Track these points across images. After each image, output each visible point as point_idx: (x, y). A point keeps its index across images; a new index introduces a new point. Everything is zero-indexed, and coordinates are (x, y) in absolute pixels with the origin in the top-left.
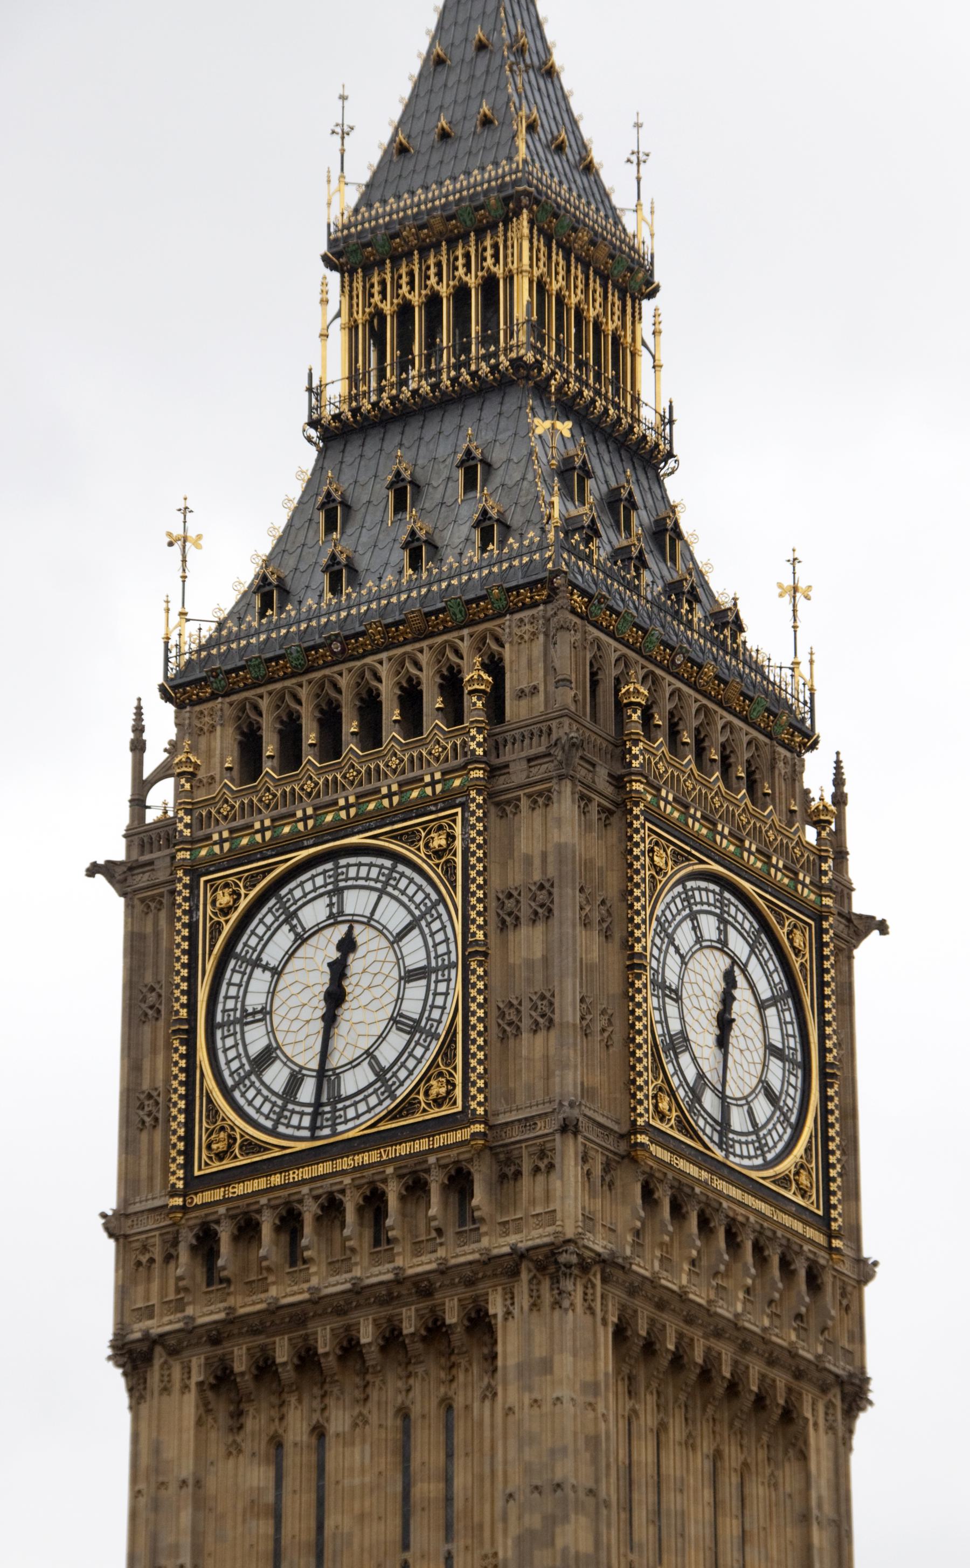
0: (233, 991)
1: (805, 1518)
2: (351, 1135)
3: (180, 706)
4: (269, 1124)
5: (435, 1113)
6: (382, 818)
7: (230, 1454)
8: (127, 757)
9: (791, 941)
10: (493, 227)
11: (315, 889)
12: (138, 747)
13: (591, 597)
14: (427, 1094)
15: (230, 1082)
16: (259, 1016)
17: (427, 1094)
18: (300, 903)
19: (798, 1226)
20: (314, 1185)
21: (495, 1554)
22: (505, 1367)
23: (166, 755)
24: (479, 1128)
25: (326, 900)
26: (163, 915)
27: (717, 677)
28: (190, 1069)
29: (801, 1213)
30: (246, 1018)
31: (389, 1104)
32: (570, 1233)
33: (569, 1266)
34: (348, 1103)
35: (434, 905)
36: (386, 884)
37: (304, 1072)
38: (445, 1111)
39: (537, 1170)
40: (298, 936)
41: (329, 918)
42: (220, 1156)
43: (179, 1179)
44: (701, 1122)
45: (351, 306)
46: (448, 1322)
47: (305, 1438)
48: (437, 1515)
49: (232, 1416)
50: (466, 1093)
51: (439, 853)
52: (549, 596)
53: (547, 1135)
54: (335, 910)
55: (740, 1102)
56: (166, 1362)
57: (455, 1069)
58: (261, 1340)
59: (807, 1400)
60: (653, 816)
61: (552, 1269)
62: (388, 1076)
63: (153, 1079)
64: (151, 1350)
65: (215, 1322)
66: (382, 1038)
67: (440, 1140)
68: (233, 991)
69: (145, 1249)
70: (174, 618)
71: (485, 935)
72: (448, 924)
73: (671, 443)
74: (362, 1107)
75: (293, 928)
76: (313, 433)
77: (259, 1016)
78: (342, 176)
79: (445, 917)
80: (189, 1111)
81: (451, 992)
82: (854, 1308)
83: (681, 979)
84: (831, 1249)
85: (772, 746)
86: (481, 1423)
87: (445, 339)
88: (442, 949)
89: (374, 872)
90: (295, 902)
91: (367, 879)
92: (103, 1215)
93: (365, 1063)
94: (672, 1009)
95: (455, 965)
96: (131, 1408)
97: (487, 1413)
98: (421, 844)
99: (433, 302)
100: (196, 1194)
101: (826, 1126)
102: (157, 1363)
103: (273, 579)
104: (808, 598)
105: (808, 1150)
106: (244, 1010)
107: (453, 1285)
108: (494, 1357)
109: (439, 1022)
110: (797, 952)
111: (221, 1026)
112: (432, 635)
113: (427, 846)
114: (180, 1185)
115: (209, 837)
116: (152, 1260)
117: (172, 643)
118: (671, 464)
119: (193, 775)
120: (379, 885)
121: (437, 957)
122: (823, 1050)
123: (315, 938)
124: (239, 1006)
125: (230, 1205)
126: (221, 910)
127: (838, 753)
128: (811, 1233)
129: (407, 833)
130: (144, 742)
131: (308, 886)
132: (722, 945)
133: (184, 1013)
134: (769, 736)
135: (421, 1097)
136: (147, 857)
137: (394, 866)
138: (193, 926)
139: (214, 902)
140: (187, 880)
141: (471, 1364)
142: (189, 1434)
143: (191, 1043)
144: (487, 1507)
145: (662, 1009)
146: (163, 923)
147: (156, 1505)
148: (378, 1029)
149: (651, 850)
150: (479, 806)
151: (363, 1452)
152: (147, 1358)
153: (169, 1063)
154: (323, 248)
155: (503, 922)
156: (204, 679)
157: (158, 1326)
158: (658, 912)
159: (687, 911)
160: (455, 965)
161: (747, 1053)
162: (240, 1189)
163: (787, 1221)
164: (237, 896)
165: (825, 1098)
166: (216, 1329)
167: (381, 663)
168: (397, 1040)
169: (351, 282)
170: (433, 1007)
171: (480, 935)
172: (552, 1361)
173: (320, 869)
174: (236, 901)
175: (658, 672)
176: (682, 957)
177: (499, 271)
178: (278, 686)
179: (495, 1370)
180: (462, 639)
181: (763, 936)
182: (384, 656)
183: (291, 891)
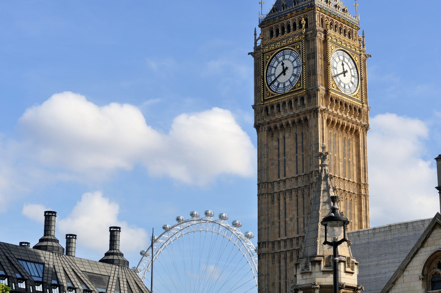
0: (269, 71)
3: (261, 28)
4: (275, 91)
5: (298, 89)
8: (254, 36)
9: (355, 59)
11: (281, 55)
12: (255, 34)
13: (321, 8)
14: (297, 86)
16: (273, 75)
17: (297, 86)
19: (357, 103)
21: (309, 154)
22: (310, 126)
24: (305, 91)
28: (264, 83)
29: (357, 101)
30: (271, 75)
31: (292, 87)
34: (286, 87)
35: (298, 57)
36: (291, 54)
38: (300, 88)
39: (314, 96)
40: (278, 62)
42: (268, 96)
44: (340, 88)
47: (282, 138)
49: (272, 135)
50: (303, 86)
51: (298, 49)
53: (315, 91)
56: (262, 127)
57: (301, 82)
60: (331, 41)
61: (316, 112)
63: (259, 85)
64: (260, 125)
65: (268, 121)
66: (291, 77)
67: (299, 93)
68: (269, 71)
69: (258, 110)
70: (260, 15)
71: (305, 61)
72: (300, 60)
74: (288, 88)
75: (278, 61)
77: (273, 75)
79: (299, 59)
80: (263, 90)
83: (337, 66)
85: (353, 29)
86: (307, 134)
88: (299, 63)
90: (278, 57)
91: (288, 53)
92: (252, 106)
95: (301, 66)
96: (257, 134)
98: (296, 47)
102: (261, 127)
103: (275, 8)
106: (271, 74)
109: (299, 74)
110: (356, 61)
111: (268, 76)
113: (296, 48)
114: (262, 101)
115: (265, 48)
116: (259, 112)
117: (260, 18)
119: (263, 39)
120: (290, 54)
122: (361, 76)
128: (359, 103)
130: (256, 34)
131: (280, 55)
133: (262, 75)
134: (352, 28)
136: (257, 51)
137: (292, 51)
138: (263, 62)
139: (266, 58)
140: (262, 55)
142: (266, 138)
143: (263, 79)
144: (308, 147)
148: (290, 76)
149: (331, 47)
151: (290, 139)
152: (259, 126)
157: (260, 122)
159: (338, 56)
161: (348, 77)
162: (271, 101)
163: (355, 102)
167: (290, 20)
168: (293, 77)
170: (298, 72)
171: (304, 61)
172: (317, 125)
173: (281, 52)
175: (333, 19)
176: (337, 63)
178: (275, 24)
180: (302, 16)
181: (351, 59)
182: (290, 19)
183: (277, 56)
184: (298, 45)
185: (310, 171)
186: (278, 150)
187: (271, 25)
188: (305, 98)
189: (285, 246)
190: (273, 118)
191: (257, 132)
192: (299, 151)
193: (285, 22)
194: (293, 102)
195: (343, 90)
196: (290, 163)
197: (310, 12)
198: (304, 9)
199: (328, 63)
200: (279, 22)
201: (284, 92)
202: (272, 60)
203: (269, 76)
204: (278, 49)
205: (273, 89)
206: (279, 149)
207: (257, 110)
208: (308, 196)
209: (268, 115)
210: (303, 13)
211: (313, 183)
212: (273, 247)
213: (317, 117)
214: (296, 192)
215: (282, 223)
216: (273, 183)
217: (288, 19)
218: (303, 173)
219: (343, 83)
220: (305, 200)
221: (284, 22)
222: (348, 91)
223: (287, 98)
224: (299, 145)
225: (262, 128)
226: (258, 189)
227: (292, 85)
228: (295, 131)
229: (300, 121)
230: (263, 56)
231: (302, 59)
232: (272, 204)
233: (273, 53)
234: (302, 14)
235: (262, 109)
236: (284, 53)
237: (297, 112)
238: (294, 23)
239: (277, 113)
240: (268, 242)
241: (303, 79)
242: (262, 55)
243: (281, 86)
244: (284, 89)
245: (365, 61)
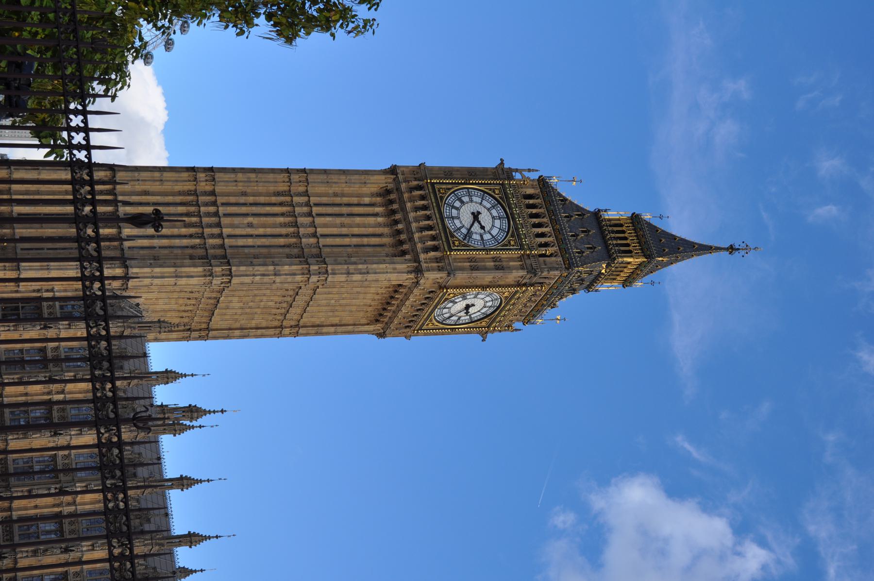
0: (476, 193)
1: (354, 325)
3: (538, 180)
4: (447, 202)
5: (451, 242)
6: (517, 229)
10: (643, 252)
12: (529, 170)
13: (566, 277)
15: (456, 193)
19: (420, 324)
24: (448, 253)
25: (498, 215)
27: (543, 304)
29: (423, 324)
30: (470, 196)
32: (425, 275)
33: (418, 274)
35: (497, 242)
36: (502, 230)
38: (452, 245)
39: (439, 267)
42: (439, 191)
48: (360, 243)
49: (380, 193)
51: (509, 242)
59: (381, 325)
61: (416, 270)
68: (476, 193)
69: (417, 173)
72: (493, 245)
73: (592, 291)
74: (451, 224)
75: (491, 208)
79: (495, 244)
80: (449, 183)
82: (400, 335)
83: (479, 298)
84: (414, 330)
87: (619, 242)
89: (504, 227)
91: (503, 225)
92: (425, 163)
93: (461, 225)
94: (472, 296)
99: (626, 238)
101: (442, 329)
105: (437, 325)
106: (472, 196)
110: (481, 323)
111: (468, 191)
112: (557, 240)
113: (511, 240)
114: (433, 181)
118: (587, 291)
119: (524, 184)
122: (458, 328)
128: (419, 326)
131: (500, 211)
132: (485, 307)
133: (471, 182)
136: (505, 173)
140: (501, 182)
145: (473, 294)
146: (490, 177)
152: (392, 174)
154: (637, 213)
156: (545, 186)
157: (400, 177)
158: (494, 293)
160: (484, 247)
162: (432, 195)
165: (448, 329)
171: (492, 253)
174: (497, 194)
177: (633, 254)
178: (544, 204)
179: (393, 257)
188: (437, 253)
189: (208, 213)
192: (355, 241)
194: (430, 233)
195: (442, 306)
197: (562, 260)
201: (445, 218)
205: (450, 200)
208: (287, 255)
211: (308, 264)
212: (205, 192)
214: (294, 233)
215: (244, 210)
217: (552, 224)
219: (453, 305)
220: (281, 250)
224: (365, 241)
229: (401, 243)
233: (503, 201)
236: (503, 218)
240: (214, 185)
241: (465, 250)
242: (501, 182)
243: (454, 212)
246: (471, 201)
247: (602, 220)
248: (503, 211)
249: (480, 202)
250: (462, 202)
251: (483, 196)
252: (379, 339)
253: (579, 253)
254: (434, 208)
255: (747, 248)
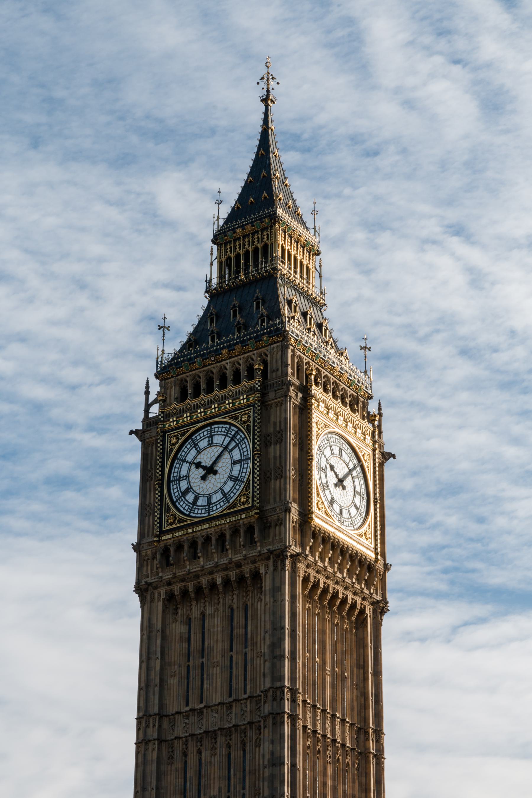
2: (215, 515)
4: (187, 513)
5: (242, 507)
7: (173, 622)
8: (143, 397)
9: (364, 457)
12: (147, 393)
15: (175, 500)
16: (185, 478)
17: (240, 501)
18: (199, 441)
20: (201, 532)
22: (265, 590)
23: (156, 396)
24: (256, 511)
25: (207, 439)
26: (154, 447)
28: (162, 496)
30: (180, 479)
34: (214, 505)
35: (243, 439)
36: (227, 433)
37: (199, 495)
40: (198, 451)
41: (208, 445)
42: (171, 524)
43: (157, 531)
45: (220, 256)
46: (246, 576)
51: (245, 422)
52: (283, 339)
53: (280, 513)
54: (210, 442)
55: (346, 508)
56: (152, 592)
57: (249, 492)
58: (184, 584)
61: (281, 557)
62: (227, 496)
64: (148, 588)
66: (225, 483)
67: (244, 516)
69: (146, 555)
71: (260, 448)
72: (248, 445)
73: (325, 301)
74: (218, 506)
75: (196, 449)
76: (206, 294)
77: (185, 478)
78: (218, 216)
79: (247, 443)
80: (161, 510)
81: (249, 467)
85: (357, 396)
86: (257, 609)
88: (246, 453)
89: (223, 430)
90: (197, 440)
91: (221, 432)
92: (133, 544)
93: (220, 492)
95: (250, 458)
96: (141, 607)
97: (259, 606)
98: (239, 419)
100: (163, 536)
102: (149, 592)
103: (192, 339)
104: (370, 350)
106: (180, 476)
107: (248, 563)
108: (261, 587)
109: (244, 477)
111: (172, 481)
113: (241, 420)
114: (158, 533)
116: (148, 559)
118: (325, 307)
120: (225, 434)
121: (244, 456)
123: (204, 452)
124: (178, 475)
125: (174, 539)
126: (173, 444)
127: (379, 400)
129: (234, 416)
131: (202, 435)
133: (160, 477)
135: (238, 502)
136: (149, 428)
137: (230, 427)
138: (163, 449)
139: (170, 441)
140: (162, 434)
141: (254, 590)
143: (162, 486)
146: (154, 450)
147: (149, 638)
148: (223, 481)
150: (258, 406)
152: (146, 590)
153: (155, 494)
155: (266, 444)
159: (329, 444)
162: (177, 534)
164: (178, 439)
166: (169, 581)
167: (227, 363)
168: (230, 484)
169: (221, 248)
170: (242, 472)
173: (206, 429)
174: (178, 441)
177: (268, 242)
178: (193, 372)
182: (228, 361)
183: (196, 437)
184: (246, 414)
185: (262, 689)
186: (187, 643)
187: (183, 373)
190: (179, 572)
191: (141, 603)
193: (215, 368)
196: (215, 672)
197: (272, 346)
198: (261, 340)
199: (309, 456)
200: (203, 367)
201: (209, 515)
202: (184, 447)
203: (175, 481)
204: (198, 422)
205: (184, 509)
206: (189, 640)
207: (143, 554)
208: (256, 747)
209: (167, 566)
210: (257, 349)
213: (281, 570)
216: (172, 717)
217: (222, 361)
218: (245, 695)
221: (214, 368)
222: (347, 523)
223: (216, 528)
225: (153, 593)
226: (138, 730)
227: (227, 500)
228: (230, 602)
229: (241, 579)
230: (164, 437)
231: (254, 443)
232: (169, 764)
233: (187, 432)
234: (255, 350)
235: (154, 551)
236: (211, 431)
237: (237, 559)
238: (235, 370)
239: (189, 560)
243: (202, 502)
244: (209, 507)
245: (381, 465)
246: (187, 477)
247: (220, 287)
248: (202, 431)
249: (188, 464)
250: (187, 491)
251: (180, 460)
252: (389, 610)
253: (263, 321)
254: (196, 532)
255: (267, 78)
